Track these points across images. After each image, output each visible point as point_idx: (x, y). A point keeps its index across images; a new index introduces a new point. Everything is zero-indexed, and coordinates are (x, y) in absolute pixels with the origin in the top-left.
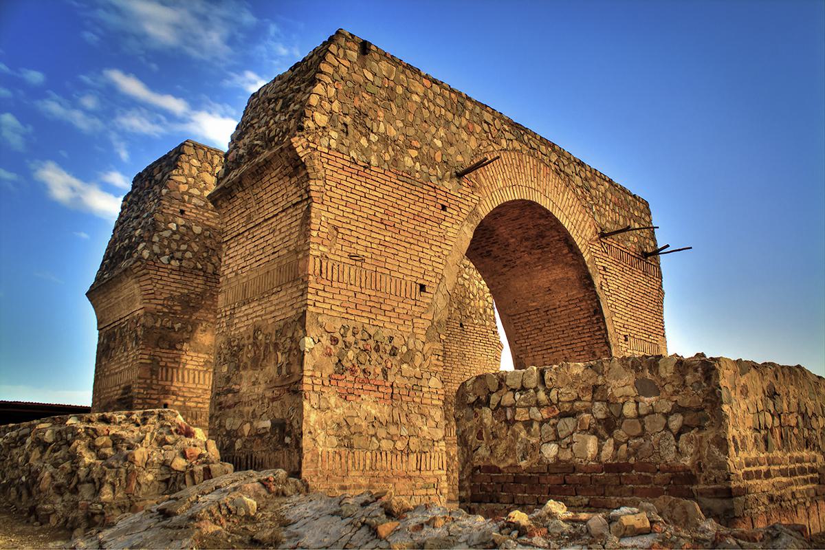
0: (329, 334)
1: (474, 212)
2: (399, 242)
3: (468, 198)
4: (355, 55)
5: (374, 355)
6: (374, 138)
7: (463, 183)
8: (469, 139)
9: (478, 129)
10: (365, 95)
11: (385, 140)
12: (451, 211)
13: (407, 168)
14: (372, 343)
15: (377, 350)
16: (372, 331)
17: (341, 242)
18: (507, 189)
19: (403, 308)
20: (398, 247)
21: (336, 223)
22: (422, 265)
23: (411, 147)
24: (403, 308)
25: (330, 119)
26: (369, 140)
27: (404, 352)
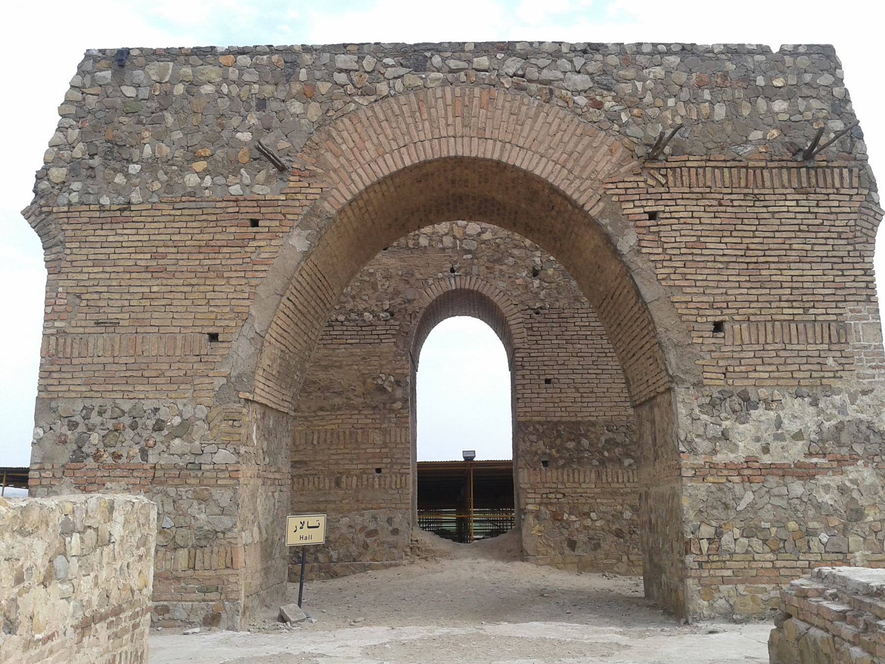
0: (67, 420)
1: (314, 212)
2: (173, 289)
3: (299, 196)
4: (108, 74)
5: (129, 433)
6: (134, 169)
7: (292, 178)
8: (306, 109)
9: (324, 87)
10: (122, 119)
11: (151, 166)
12: (268, 223)
13: (189, 190)
14: (126, 420)
15: (134, 427)
16: (126, 406)
17: (86, 310)
18: (387, 156)
19: (179, 369)
20: (171, 296)
21: (77, 290)
22: (211, 309)
23: (197, 158)
24: (179, 369)
25: (71, 170)
26: (127, 175)
27: (175, 424)
